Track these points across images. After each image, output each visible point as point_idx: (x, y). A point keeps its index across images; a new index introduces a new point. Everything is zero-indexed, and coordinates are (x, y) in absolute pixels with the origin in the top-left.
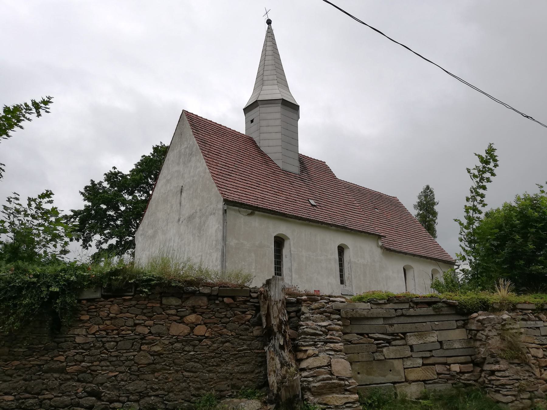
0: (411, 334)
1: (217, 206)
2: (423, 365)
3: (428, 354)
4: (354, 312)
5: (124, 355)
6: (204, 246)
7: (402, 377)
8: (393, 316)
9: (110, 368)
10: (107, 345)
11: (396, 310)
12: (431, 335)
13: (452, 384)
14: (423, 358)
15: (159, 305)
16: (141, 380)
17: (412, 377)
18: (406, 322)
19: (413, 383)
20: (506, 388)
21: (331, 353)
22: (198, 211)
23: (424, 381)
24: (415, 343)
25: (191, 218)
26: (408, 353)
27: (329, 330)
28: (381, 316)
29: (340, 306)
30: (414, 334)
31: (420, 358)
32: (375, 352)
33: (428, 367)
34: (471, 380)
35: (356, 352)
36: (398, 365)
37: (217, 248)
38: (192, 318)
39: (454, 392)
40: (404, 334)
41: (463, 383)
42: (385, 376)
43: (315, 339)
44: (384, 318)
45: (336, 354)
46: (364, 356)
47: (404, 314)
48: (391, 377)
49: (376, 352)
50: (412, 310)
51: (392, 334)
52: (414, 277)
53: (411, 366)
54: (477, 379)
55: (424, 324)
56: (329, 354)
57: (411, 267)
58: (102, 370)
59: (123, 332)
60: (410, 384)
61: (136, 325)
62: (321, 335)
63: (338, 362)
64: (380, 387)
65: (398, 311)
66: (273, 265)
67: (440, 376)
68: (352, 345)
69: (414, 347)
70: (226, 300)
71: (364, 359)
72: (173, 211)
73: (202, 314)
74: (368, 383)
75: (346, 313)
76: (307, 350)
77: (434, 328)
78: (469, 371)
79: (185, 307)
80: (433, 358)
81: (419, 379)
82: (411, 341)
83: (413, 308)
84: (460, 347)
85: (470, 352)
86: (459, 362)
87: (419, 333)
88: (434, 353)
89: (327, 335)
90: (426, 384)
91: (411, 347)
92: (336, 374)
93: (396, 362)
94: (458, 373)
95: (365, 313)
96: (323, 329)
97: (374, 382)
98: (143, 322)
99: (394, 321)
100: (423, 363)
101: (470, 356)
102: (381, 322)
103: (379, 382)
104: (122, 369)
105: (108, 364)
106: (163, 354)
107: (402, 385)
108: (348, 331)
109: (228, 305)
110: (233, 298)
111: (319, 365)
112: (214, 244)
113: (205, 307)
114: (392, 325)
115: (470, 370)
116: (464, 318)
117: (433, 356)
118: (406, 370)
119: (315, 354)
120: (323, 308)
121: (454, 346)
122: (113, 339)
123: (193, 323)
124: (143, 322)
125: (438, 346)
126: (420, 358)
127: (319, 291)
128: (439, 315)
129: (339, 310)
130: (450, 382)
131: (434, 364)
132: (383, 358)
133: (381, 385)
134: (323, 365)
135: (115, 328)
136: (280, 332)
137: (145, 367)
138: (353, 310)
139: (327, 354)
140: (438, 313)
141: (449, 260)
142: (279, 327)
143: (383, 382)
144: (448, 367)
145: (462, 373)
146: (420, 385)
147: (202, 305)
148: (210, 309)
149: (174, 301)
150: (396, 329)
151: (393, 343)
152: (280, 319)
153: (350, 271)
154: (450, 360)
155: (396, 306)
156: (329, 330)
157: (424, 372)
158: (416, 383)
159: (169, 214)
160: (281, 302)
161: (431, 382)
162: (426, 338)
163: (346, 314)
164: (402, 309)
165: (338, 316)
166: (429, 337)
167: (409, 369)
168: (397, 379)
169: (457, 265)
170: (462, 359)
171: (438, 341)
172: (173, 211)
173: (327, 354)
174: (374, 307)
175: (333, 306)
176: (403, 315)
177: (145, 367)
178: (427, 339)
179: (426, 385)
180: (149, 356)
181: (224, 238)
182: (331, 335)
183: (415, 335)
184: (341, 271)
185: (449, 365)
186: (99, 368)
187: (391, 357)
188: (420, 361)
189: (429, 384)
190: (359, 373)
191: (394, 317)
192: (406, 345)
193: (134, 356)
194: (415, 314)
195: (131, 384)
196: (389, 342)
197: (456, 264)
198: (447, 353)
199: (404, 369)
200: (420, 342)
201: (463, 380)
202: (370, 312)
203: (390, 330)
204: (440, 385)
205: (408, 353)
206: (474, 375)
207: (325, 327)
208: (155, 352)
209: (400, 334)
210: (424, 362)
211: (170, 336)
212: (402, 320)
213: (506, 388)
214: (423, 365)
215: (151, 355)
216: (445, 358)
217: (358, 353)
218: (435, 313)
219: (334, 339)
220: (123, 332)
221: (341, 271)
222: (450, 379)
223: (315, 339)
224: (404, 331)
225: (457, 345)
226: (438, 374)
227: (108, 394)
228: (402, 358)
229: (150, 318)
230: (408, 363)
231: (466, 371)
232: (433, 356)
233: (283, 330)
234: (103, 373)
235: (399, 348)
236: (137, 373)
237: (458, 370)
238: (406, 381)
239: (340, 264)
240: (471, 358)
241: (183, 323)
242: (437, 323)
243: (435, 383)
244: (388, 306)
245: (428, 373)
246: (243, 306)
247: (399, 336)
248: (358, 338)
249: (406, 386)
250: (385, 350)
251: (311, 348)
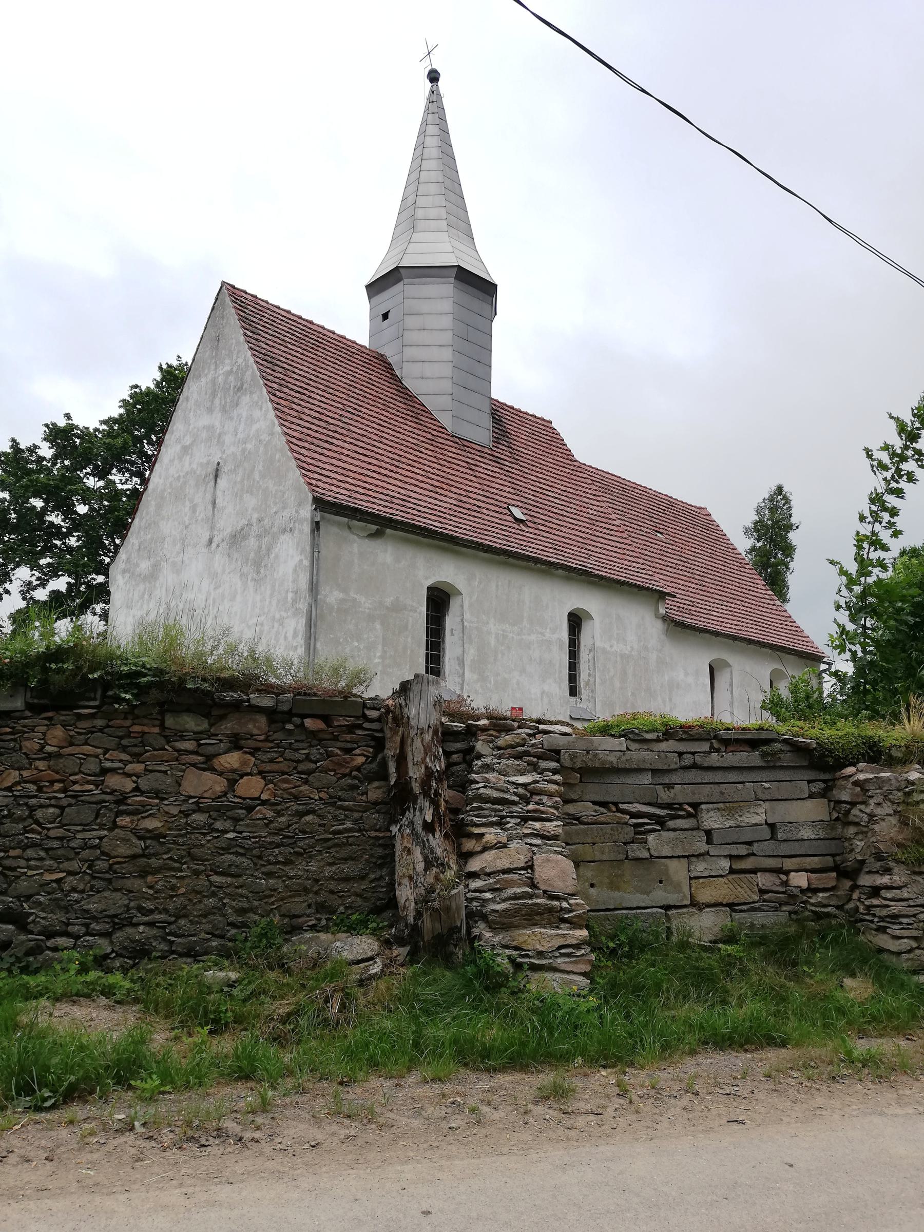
0: (711, 806)
1: (297, 512)
2: (732, 871)
3: (743, 850)
4: (590, 756)
5: (79, 836)
6: (267, 603)
7: (684, 896)
8: (673, 766)
9: (47, 863)
10: (39, 814)
11: (680, 754)
12: (752, 810)
13: (790, 913)
14: (731, 857)
15: (156, 730)
16: (116, 890)
17: (705, 896)
18: (700, 781)
19: (708, 910)
20: (901, 923)
21: (533, 841)
22: (254, 521)
23: (731, 906)
24: (717, 826)
25: (237, 539)
26: (703, 847)
27: (533, 793)
28: (648, 766)
29: (561, 744)
30: (715, 805)
31: (725, 856)
32: (629, 843)
33: (742, 876)
34: (830, 906)
35: (589, 840)
36: (678, 870)
37: (297, 609)
38: (232, 760)
39: (792, 929)
40: (696, 806)
41: (812, 911)
42: (648, 893)
43: (501, 811)
44: (655, 772)
45: (546, 844)
46: (607, 850)
47: (699, 763)
48: (661, 895)
49: (633, 842)
50: (714, 755)
51: (669, 806)
52: (731, 685)
53: (706, 874)
54: (843, 905)
55: (740, 786)
56: (531, 845)
57: (727, 665)
58: (29, 868)
59: (77, 787)
60: (700, 910)
61: (104, 771)
62: (515, 803)
63: (548, 860)
64: (636, 916)
65: (685, 756)
66: (423, 651)
67: (766, 897)
68: (582, 826)
69: (715, 835)
70: (308, 722)
71: (605, 857)
73: (254, 752)
74: (612, 907)
75: (573, 757)
76: (483, 835)
77: (760, 796)
78: (826, 886)
79: (217, 735)
80: (752, 858)
81: (720, 900)
82: (709, 821)
83: (718, 751)
84: (813, 837)
85: (832, 847)
86: (808, 867)
87: (728, 805)
88: (755, 848)
89: (528, 803)
90: (735, 911)
91: (708, 833)
92: (543, 887)
93: (673, 865)
94: (803, 891)
95: (612, 758)
96: (521, 791)
97: (624, 905)
98: (121, 765)
99: (675, 778)
100: (731, 867)
101: (833, 855)
102: (647, 779)
103: (635, 906)
104: (75, 865)
105: (42, 854)
106: (165, 837)
107: (684, 913)
108: (574, 796)
109: (313, 734)
110: (326, 719)
111: (507, 866)
112: (289, 599)
113: (262, 738)
114: (669, 786)
115: (830, 886)
116: (826, 776)
117: (754, 854)
118: (693, 882)
119: (500, 842)
120: (523, 746)
121: (800, 833)
122: (53, 802)
123: (234, 771)
124: (121, 765)
125: (767, 833)
126: (725, 856)
127: (521, 709)
128: (774, 767)
129: (558, 752)
130: (784, 908)
131: (754, 871)
132: (647, 855)
133: (638, 911)
134: (515, 866)
135: (58, 777)
136: (426, 794)
137: (125, 862)
138: (588, 753)
139: (526, 844)
140: (772, 764)
141: (810, 650)
142: (425, 783)
143: (643, 905)
144: (784, 877)
145: (812, 890)
146: (721, 914)
147: (255, 732)
148: (272, 741)
149: (191, 723)
150: (679, 794)
151: (671, 824)
152: (427, 768)
153: (592, 667)
154: (788, 864)
155: (682, 747)
156: (533, 793)
157: (731, 886)
158: (713, 909)
159: (187, 527)
160: (431, 731)
161: (745, 907)
162: (740, 816)
163: (571, 760)
164: (693, 753)
165: (554, 765)
166: (748, 815)
167: (701, 881)
168: (672, 899)
169: (826, 663)
170: (815, 862)
171: (766, 823)
173: (526, 844)
174: (633, 746)
175: (545, 743)
176: (695, 766)
177: (125, 862)
178: (744, 818)
179: (733, 914)
180: (135, 840)
181: (314, 588)
182: (537, 803)
183: (718, 809)
184: (573, 667)
185: (787, 873)
186: (22, 863)
187: (664, 854)
188: (725, 864)
189: (742, 911)
190: (592, 885)
191: (676, 770)
192: (698, 829)
193: (101, 838)
194: (722, 765)
195: (94, 899)
196: (661, 822)
197: (825, 660)
198: (784, 849)
199: (691, 878)
200: (728, 824)
201: (813, 905)
202: (624, 758)
203: (664, 796)
204: (765, 914)
205: (703, 847)
206: (837, 896)
207: (524, 786)
208: (148, 831)
209: (686, 807)
210: (734, 867)
211: (182, 798)
212: (692, 776)
213: (901, 923)
214: (732, 871)
215: (140, 838)
216: (780, 860)
217: (594, 844)
218: (764, 764)
219: (542, 812)
220: (77, 787)
221: (573, 667)
222: (787, 904)
223: (501, 811)
224: (695, 799)
225: (806, 833)
226: (762, 892)
227: (41, 918)
228: (687, 857)
229: (137, 757)
230: (700, 867)
231: (821, 886)
232: (754, 854)
233: (433, 791)
234: (30, 873)
235: (682, 835)
236: (107, 876)
237: (804, 884)
238: (694, 904)
239: (570, 651)
240: (834, 861)
241: (212, 770)
242: (766, 785)
243: (754, 909)
244: (664, 746)
245: (740, 889)
246: (348, 737)
247: (685, 810)
248: (595, 811)
249: (692, 915)
250: (651, 837)
251: (492, 830)
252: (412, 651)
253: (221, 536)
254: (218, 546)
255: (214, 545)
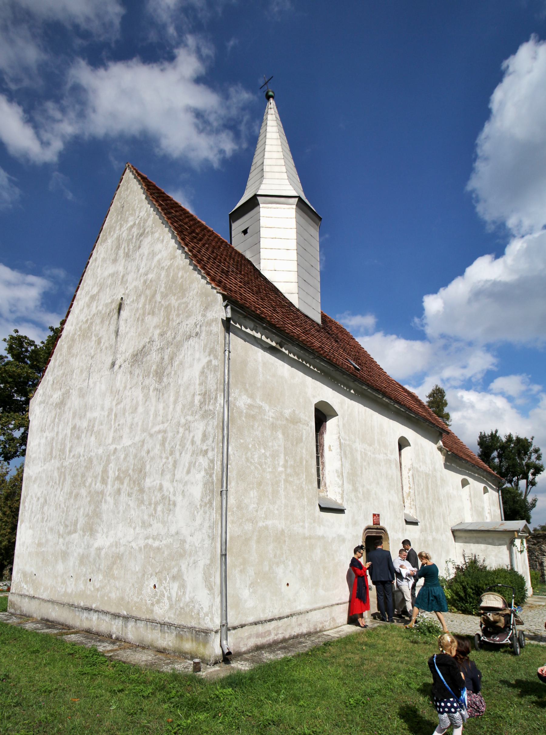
72: (101, 350)
172: (101, 350)
252: (307, 462)
253: (123, 358)
254: (120, 366)
255: (116, 367)
